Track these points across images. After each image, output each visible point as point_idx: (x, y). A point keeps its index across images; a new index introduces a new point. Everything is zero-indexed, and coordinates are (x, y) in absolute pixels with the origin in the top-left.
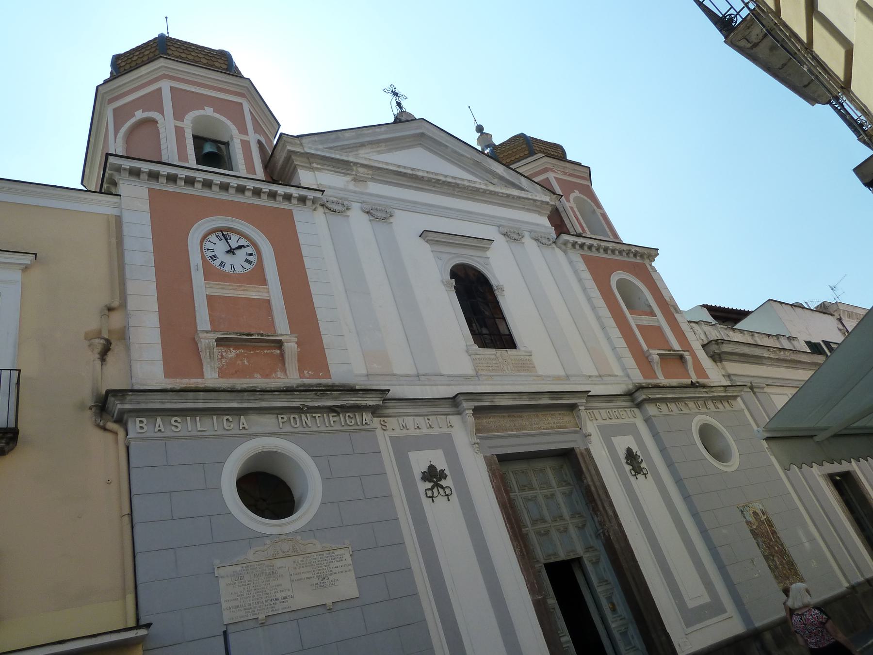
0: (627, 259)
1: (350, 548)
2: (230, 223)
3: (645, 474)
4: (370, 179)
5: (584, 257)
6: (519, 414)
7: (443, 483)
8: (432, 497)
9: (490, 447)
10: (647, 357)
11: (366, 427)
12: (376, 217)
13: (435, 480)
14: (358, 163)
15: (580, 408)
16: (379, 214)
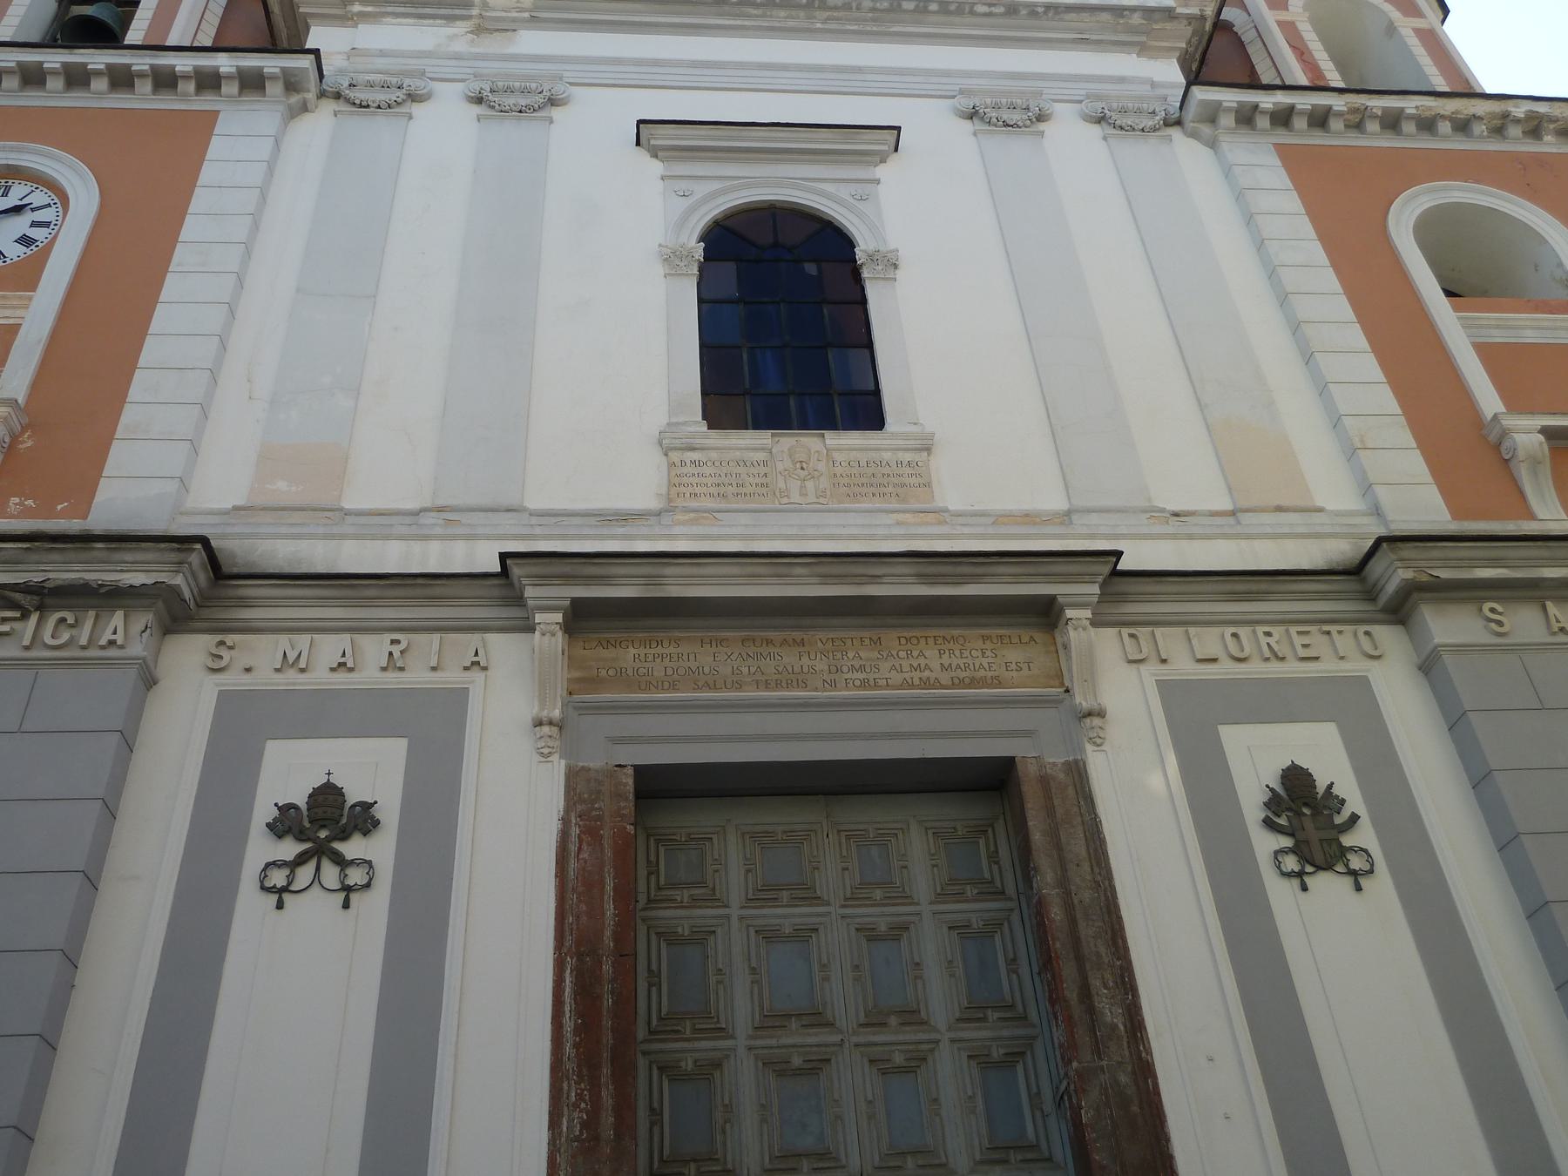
0: (1494, 146)
3: (1354, 874)
5: (1283, 151)
6: (797, 635)
10: (1497, 447)
11: (112, 652)
15: (1069, 613)
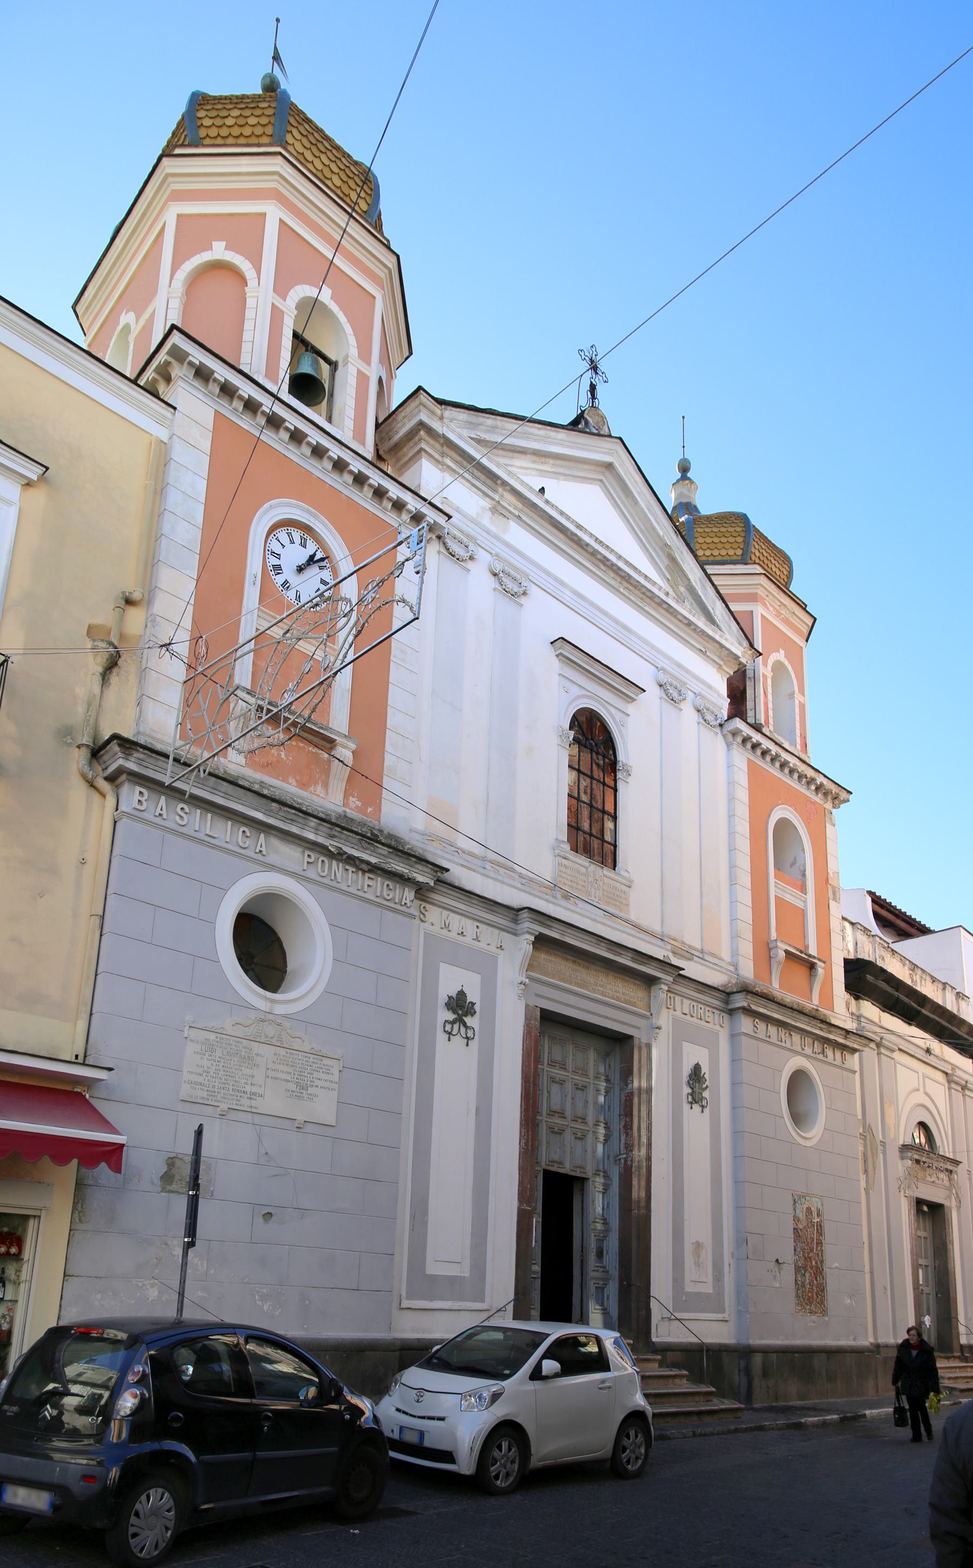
1: (341, 1061)
2: (312, 519)
4: (515, 516)
7: (468, 1020)
8: (450, 1033)
9: (537, 995)
12: (504, 586)
13: (460, 1012)
14: (508, 484)
16: (510, 585)
